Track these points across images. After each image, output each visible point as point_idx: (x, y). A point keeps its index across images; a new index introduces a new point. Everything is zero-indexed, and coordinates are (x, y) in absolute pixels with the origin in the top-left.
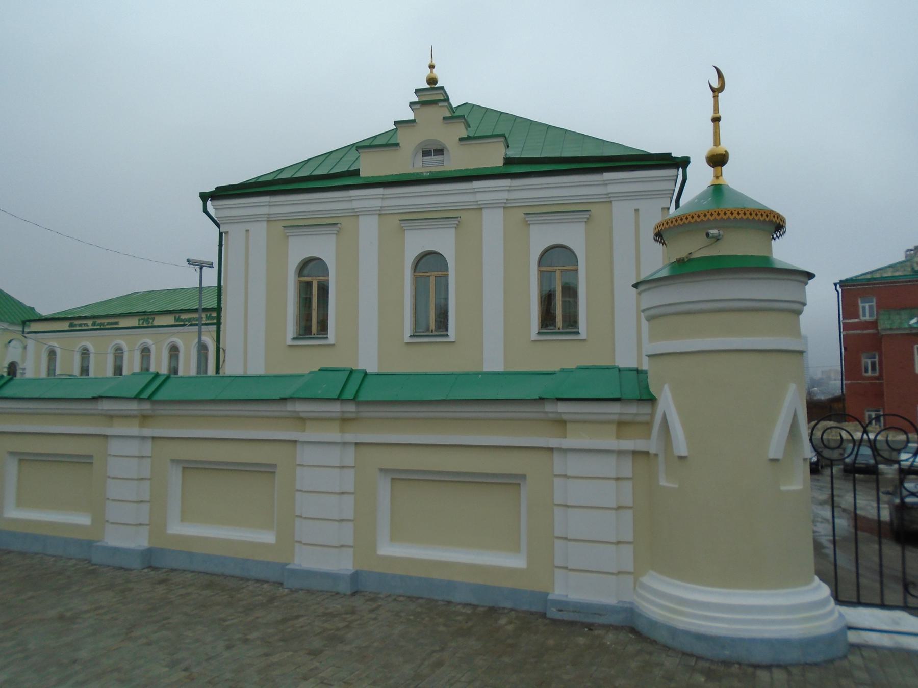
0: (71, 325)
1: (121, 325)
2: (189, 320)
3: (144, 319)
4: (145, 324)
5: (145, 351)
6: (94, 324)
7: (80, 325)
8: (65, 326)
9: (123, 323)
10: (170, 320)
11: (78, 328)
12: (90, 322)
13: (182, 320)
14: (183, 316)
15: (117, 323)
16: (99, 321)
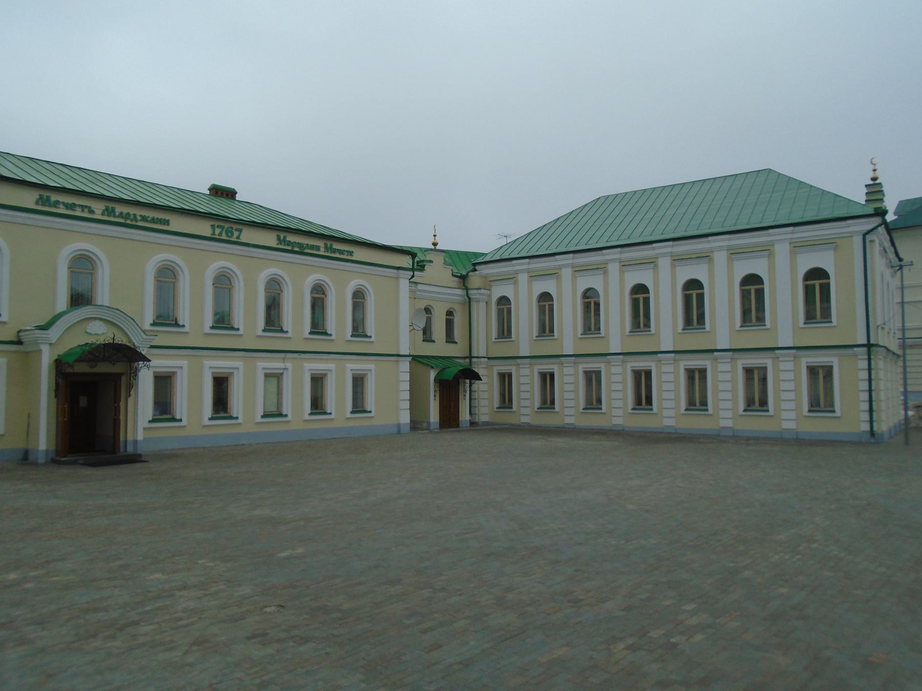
0: (43, 201)
1: (172, 227)
2: (300, 245)
3: (222, 228)
4: (224, 237)
5: (223, 282)
6: (109, 212)
7: (72, 207)
8: (28, 199)
9: (178, 223)
10: (270, 239)
11: (62, 210)
12: (98, 207)
13: (289, 243)
14: (291, 238)
15: (167, 222)
16: (119, 209)
